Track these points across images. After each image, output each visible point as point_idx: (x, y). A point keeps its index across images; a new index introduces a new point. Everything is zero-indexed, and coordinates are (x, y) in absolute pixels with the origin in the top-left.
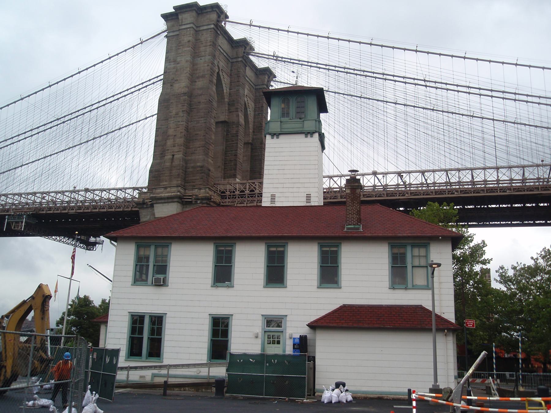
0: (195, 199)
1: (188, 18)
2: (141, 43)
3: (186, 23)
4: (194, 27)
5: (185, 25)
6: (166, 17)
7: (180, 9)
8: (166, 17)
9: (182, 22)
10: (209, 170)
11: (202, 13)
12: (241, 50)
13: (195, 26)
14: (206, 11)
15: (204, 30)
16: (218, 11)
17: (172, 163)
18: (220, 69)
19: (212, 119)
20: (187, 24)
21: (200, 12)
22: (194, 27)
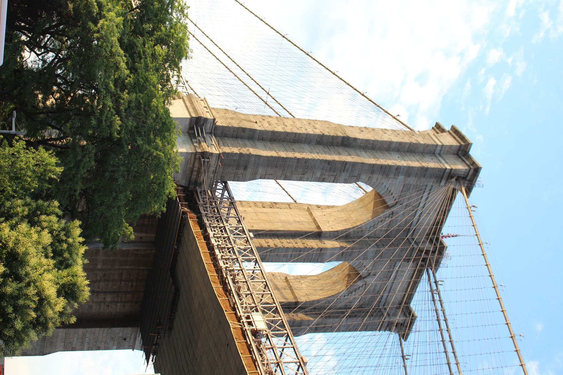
0: (199, 140)
1: (448, 140)
2: (394, 118)
3: (440, 140)
4: (439, 148)
5: (437, 138)
6: (438, 128)
7: (455, 132)
8: (438, 128)
9: (439, 136)
10: (246, 168)
11: (460, 157)
12: (427, 246)
13: (441, 151)
14: (465, 160)
15: (439, 160)
16: (470, 174)
17: (246, 120)
18: (392, 209)
19: (320, 172)
20: (439, 140)
21: (460, 155)
22: (439, 148)
